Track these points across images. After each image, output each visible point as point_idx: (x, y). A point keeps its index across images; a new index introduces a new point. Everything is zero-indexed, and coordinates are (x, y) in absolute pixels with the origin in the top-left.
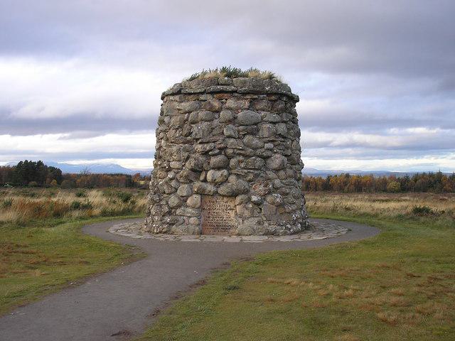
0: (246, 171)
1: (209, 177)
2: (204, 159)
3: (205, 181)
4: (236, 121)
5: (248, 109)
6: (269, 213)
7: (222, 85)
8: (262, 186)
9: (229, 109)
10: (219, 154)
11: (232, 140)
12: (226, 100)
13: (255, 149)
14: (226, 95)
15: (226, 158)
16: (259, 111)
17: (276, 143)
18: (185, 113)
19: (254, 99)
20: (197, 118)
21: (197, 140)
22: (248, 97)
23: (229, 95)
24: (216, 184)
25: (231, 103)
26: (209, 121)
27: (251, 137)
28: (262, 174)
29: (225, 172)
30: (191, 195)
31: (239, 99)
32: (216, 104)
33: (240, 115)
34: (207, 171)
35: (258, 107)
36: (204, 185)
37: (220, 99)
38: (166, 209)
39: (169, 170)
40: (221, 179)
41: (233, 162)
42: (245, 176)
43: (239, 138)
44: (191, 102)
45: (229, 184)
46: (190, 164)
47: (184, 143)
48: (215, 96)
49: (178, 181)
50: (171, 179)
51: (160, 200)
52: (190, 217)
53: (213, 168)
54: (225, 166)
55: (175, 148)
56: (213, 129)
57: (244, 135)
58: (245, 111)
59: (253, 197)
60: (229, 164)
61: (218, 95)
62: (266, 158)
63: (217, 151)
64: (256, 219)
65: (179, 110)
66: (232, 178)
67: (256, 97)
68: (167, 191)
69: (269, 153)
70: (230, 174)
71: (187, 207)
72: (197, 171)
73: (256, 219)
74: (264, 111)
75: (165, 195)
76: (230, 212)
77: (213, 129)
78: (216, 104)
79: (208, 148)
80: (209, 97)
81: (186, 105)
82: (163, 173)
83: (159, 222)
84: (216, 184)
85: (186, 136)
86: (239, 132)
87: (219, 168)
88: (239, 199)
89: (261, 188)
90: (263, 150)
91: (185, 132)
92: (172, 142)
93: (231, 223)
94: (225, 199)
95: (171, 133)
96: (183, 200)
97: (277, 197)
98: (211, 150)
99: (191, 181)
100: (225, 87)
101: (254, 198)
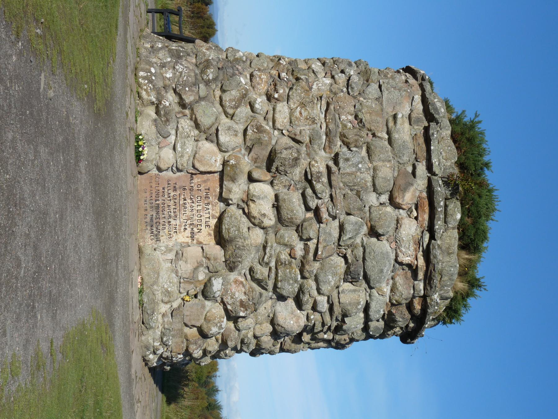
0: (273, 264)
1: (256, 188)
2: (297, 178)
5: (396, 260)
6: (188, 313)
7: (446, 206)
8: (243, 297)
10: (308, 209)
12: (416, 218)
14: (426, 217)
15: (299, 222)
16: (391, 282)
17: (327, 318)
18: (388, 133)
21: (336, 163)
22: (421, 262)
23: (426, 223)
25: (410, 229)
29: (270, 220)
30: (221, 150)
31: (419, 243)
32: (408, 198)
33: (384, 246)
34: (272, 183)
35: (400, 280)
36: (243, 179)
40: (255, 213)
42: (261, 262)
44: (411, 145)
48: (425, 194)
51: (207, 83)
55: (318, 112)
58: (393, 256)
59: (220, 280)
61: (426, 202)
63: (313, 204)
64: (173, 289)
65: (395, 117)
66: (257, 236)
67: (421, 275)
68: (227, 97)
73: (173, 289)
74: (392, 290)
75: (218, 93)
76: (188, 233)
77: (358, 194)
78: (408, 198)
79: (318, 186)
80: (421, 183)
81: (405, 132)
82: (263, 87)
83: (160, 84)
85: (343, 136)
86: (353, 246)
87: (277, 207)
89: (240, 295)
90: (315, 293)
91: (351, 137)
92: (328, 104)
93: (164, 238)
96: (213, 136)
99: (250, 150)
100: (442, 216)
101: (217, 285)
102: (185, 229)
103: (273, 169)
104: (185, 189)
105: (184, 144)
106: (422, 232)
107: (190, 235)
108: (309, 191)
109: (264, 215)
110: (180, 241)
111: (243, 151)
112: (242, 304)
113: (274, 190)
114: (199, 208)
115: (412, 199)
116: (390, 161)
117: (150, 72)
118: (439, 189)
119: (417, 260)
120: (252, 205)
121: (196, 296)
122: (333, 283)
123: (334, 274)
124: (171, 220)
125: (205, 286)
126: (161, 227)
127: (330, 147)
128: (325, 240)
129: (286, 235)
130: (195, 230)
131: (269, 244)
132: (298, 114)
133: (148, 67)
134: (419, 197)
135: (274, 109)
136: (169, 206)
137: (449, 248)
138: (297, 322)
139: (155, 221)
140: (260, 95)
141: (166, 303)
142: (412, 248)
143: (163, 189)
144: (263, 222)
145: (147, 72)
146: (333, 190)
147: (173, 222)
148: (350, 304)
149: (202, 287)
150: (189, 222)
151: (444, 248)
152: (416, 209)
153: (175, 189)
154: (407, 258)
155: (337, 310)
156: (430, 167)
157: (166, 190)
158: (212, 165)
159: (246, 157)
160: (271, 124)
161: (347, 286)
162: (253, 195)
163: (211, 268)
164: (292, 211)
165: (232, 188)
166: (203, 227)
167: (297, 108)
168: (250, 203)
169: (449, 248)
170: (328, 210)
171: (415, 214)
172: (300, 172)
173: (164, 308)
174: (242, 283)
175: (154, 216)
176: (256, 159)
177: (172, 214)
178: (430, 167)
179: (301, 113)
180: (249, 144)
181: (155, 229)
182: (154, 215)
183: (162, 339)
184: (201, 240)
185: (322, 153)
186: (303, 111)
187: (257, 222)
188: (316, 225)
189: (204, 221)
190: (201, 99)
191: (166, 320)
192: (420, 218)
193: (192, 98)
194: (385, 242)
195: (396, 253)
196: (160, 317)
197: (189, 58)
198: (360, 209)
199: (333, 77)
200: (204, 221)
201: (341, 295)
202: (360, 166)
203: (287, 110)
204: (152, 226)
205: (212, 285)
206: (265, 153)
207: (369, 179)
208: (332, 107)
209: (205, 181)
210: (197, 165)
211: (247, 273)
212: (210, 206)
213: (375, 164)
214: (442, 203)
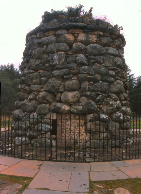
14: (77, 30)
22: (96, 33)
32: (70, 37)
34: (61, 93)
37: (73, 34)
60: (80, 87)
62: (111, 83)
67: (102, 33)
69: (112, 79)
78: (70, 37)
80: (64, 31)
87: (73, 90)
88: (89, 117)
97: (120, 116)
107: (82, 127)
109: (74, 96)
120: (70, 101)
154: (94, 38)
167: (33, 82)
168: (69, 101)
171: (76, 35)
180: (46, 101)
186: (34, 79)
192: (78, 32)
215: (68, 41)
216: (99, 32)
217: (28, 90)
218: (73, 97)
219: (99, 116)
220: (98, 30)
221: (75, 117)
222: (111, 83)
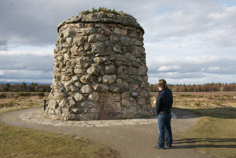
0: (127, 76)
3: (101, 82)
4: (119, 43)
5: (126, 36)
6: (142, 103)
8: (137, 85)
9: (116, 34)
10: (111, 64)
11: (119, 55)
12: (114, 28)
13: (132, 62)
14: (113, 25)
16: (131, 38)
17: (142, 59)
19: (129, 30)
20: (95, 39)
22: (126, 28)
23: (116, 25)
24: (108, 84)
25: (117, 31)
26: (102, 41)
27: (129, 54)
28: (136, 78)
29: (115, 76)
31: (121, 28)
34: (102, 76)
36: (101, 85)
38: (72, 102)
39: (74, 74)
41: (120, 69)
43: (123, 54)
45: (117, 85)
46: (90, 71)
47: (85, 56)
48: (106, 25)
49: (80, 82)
50: (76, 81)
52: (91, 108)
53: (108, 74)
54: (116, 73)
56: (106, 47)
57: (126, 52)
58: (125, 37)
60: (117, 71)
61: (108, 24)
67: (130, 28)
68: (72, 90)
70: (117, 78)
71: (89, 101)
72: (95, 76)
74: (134, 38)
76: (117, 103)
78: (108, 30)
80: (103, 26)
84: (107, 84)
85: (87, 51)
86: (122, 50)
87: (110, 74)
88: (124, 95)
94: (114, 95)
95: (74, 49)
98: (106, 61)
101: (134, 94)
102: (116, 104)
103: (98, 75)
104: (103, 104)
105: (89, 105)
106: (118, 27)
108: (106, 63)
109: (113, 78)
110: (120, 106)
111: (91, 85)
112: (139, 86)
113: (105, 75)
114: (109, 99)
115: (108, 29)
116: (96, 35)
117: (64, 116)
118: (105, 20)
119: (126, 29)
121: (137, 101)
122: (133, 57)
123: (131, 56)
124: (113, 109)
125: (134, 98)
126: (115, 112)
127: (90, 55)
128: (121, 59)
129: (119, 71)
130: (116, 101)
131: (122, 77)
132: (78, 66)
133: (62, 117)
134: (107, 27)
135: (77, 74)
136: (109, 109)
137: (123, 19)
138: (143, 68)
139: (113, 114)
140: (71, 78)
141: (139, 110)
142: (123, 30)
143: (103, 111)
144: (115, 79)
145: (64, 117)
146: (105, 55)
147: (114, 108)
148: (138, 52)
149: (135, 99)
150: (114, 103)
151: (122, 20)
152: (111, 28)
153: (104, 107)
155: (139, 56)
156: (97, 22)
157: (103, 110)
158: (96, 95)
159: (93, 84)
160: (82, 75)
161: (134, 53)
162: (107, 82)
163: (129, 96)
164: (112, 69)
165: (104, 89)
166: (116, 98)
169: (123, 19)
170: (111, 57)
172: (99, 66)
173: (140, 111)
174: (133, 86)
175: (112, 114)
176: (94, 80)
177: (111, 108)
178: (97, 22)
179: (78, 65)
181: (116, 114)
182: (111, 114)
183: (149, 111)
184: (119, 99)
185: (92, 58)
187: (114, 81)
188: (117, 62)
189: (114, 98)
190: (74, 99)
191: (144, 110)
192: (114, 27)
193: (73, 102)
194: (121, 39)
195: (124, 35)
196: (143, 112)
197: (58, 102)
198: (111, 46)
199: (64, 53)
200: (114, 98)
201: (136, 54)
202: (97, 45)
203: (77, 69)
204: (115, 115)
205: (135, 96)
206: (92, 77)
207: (101, 43)
208: (76, 54)
209: (101, 98)
210: (96, 100)
211: (130, 84)
212: (109, 96)
213: (96, 40)
214: (110, 19)
215: (106, 34)
216: (128, 27)
217: (72, 73)
218: (112, 79)
219: (131, 94)
220: (128, 26)
221: (112, 95)
222: (137, 68)
